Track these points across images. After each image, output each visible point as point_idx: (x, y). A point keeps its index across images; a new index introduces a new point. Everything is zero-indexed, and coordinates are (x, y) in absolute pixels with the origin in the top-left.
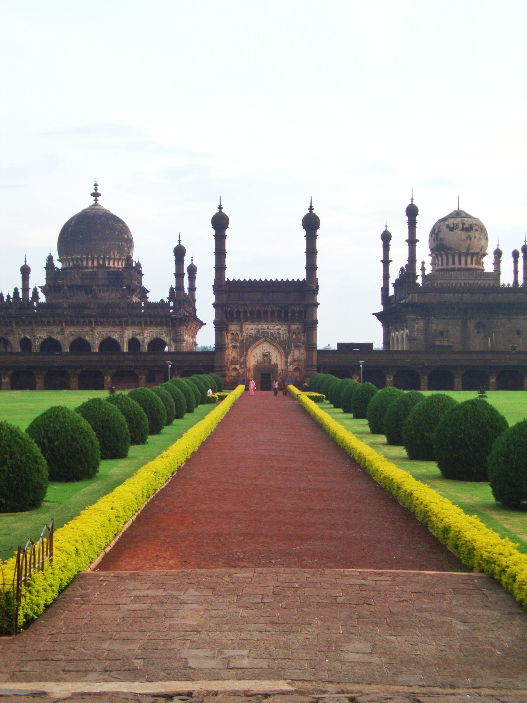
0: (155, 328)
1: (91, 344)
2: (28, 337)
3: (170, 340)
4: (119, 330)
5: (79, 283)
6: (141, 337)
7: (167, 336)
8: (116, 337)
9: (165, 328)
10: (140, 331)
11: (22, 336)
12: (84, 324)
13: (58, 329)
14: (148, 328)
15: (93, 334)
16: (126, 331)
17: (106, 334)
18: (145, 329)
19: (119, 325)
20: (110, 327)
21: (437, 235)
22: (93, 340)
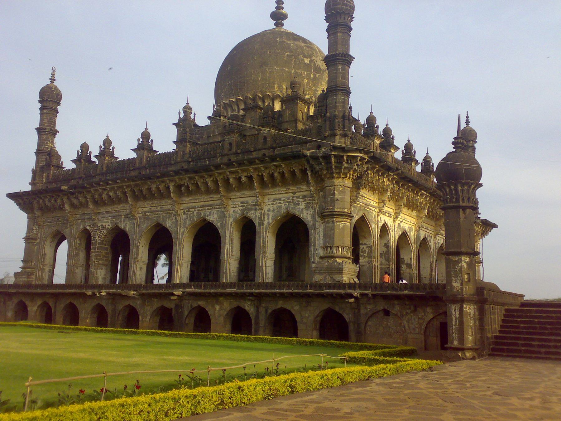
0: (283, 189)
1: (173, 235)
3: (313, 217)
6: (258, 214)
7: (307, 207)
8: (213, 217)
9: (304, 187)
12: (164, 195)
13: (123, 209)
14: (271, 190)
15: (176, 215)
16: (230, 202)
17: (199, 213)
18: (264, 195)
19: (217, 191)
20: (206, 197)
22: (177, 226)
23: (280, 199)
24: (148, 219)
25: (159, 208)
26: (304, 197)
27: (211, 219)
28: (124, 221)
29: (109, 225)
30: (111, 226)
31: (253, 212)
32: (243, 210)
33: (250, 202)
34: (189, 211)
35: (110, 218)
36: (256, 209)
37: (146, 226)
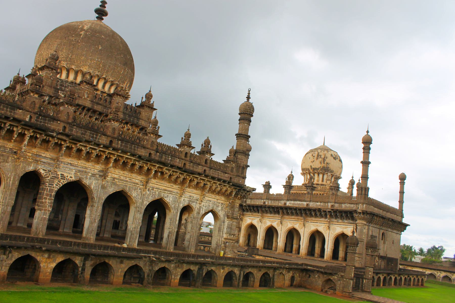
2: (42, 171)
4: (175, 191)
5: (88, 104)
6: (198, 206)
7: (222, 210)
8: (169, 199)
10: (198, 197)
11: (31, 168)
21: (324, 160)
23: (210, 201)
24: (115, 184)
25: (127, 179)
26: (222, 204)
27: (168, 201)
28: (90, 179)
29: (71, 177)
30: (73, 179)
31: (195, 204)
32: (189, 201)
33: (195, 197)
34: (153, 190)
35: (74, 171)
36: (196, 203)
37: (111, 190)
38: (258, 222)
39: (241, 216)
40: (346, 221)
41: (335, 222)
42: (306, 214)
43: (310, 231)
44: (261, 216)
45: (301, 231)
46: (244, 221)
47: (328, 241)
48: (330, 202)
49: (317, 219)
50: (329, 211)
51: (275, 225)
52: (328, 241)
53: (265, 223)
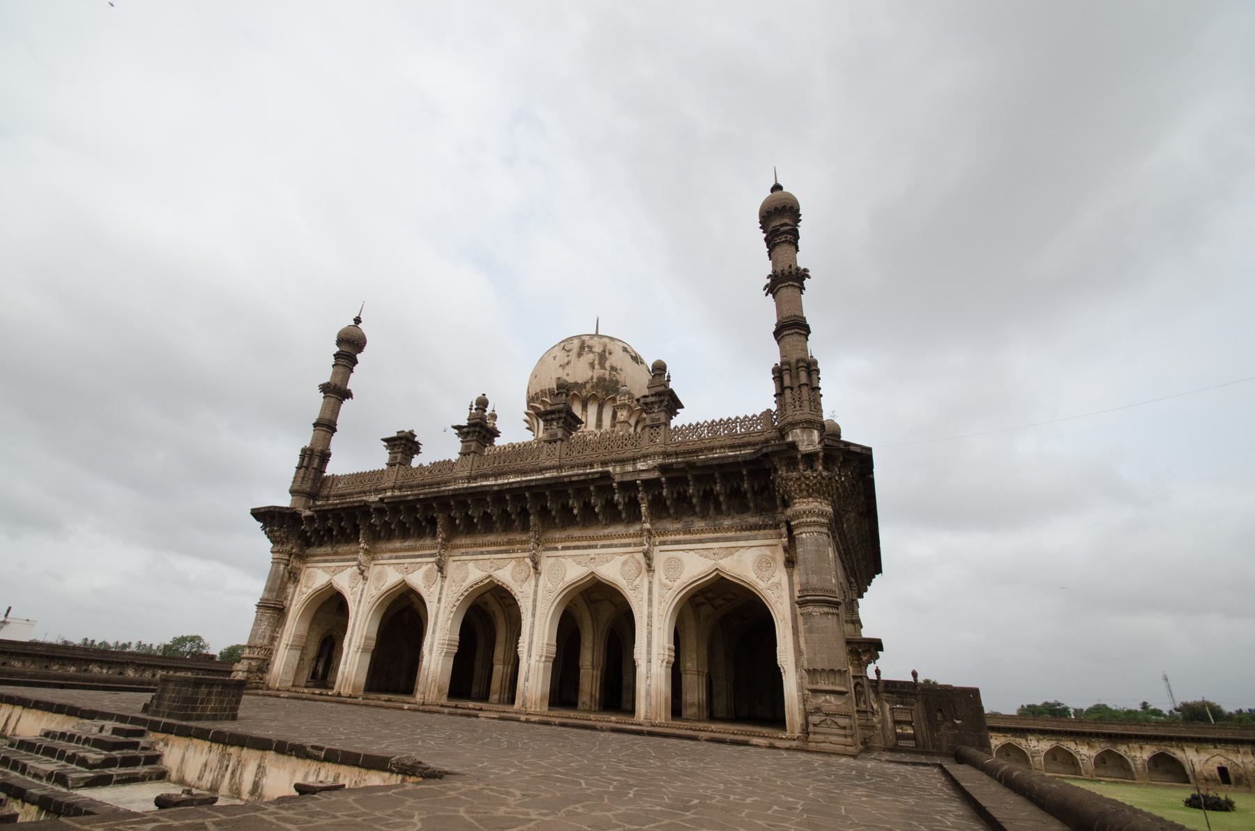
38: (353, 578)
39: (295, 563)
40: (727, 522)
41: (677, 532)
42: (544, 513)
43: (561, 586)
44: (367, 552)
45: (523, 593)
46: (303, 579)
47: (650, 625)
48: (645, 457)
49: (590, 532)
50: (645, 482)
51: (417, 580)
52: (650, 625)
53: (380, 577)
